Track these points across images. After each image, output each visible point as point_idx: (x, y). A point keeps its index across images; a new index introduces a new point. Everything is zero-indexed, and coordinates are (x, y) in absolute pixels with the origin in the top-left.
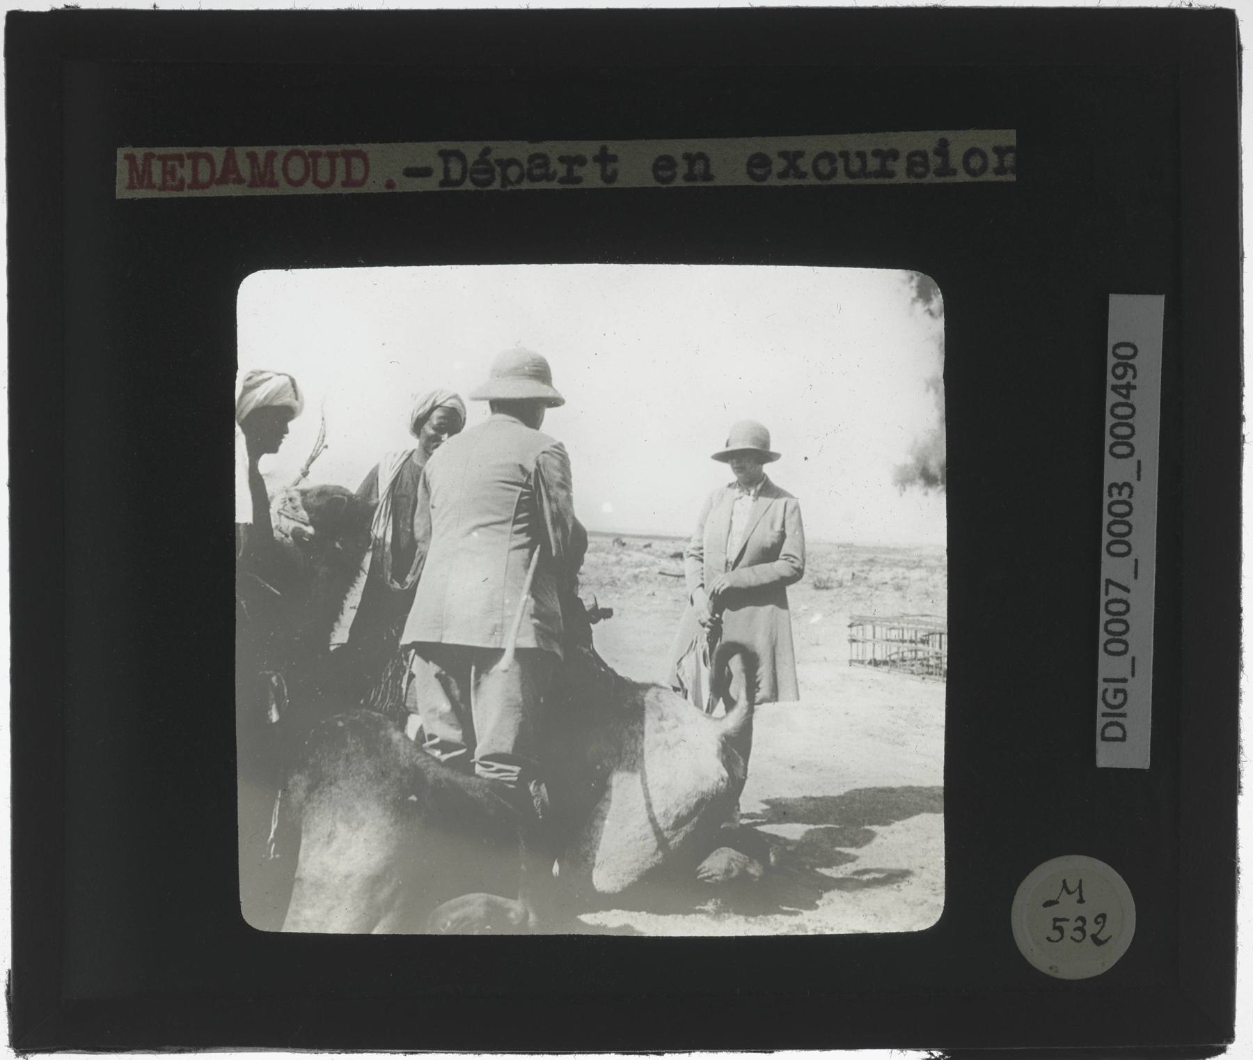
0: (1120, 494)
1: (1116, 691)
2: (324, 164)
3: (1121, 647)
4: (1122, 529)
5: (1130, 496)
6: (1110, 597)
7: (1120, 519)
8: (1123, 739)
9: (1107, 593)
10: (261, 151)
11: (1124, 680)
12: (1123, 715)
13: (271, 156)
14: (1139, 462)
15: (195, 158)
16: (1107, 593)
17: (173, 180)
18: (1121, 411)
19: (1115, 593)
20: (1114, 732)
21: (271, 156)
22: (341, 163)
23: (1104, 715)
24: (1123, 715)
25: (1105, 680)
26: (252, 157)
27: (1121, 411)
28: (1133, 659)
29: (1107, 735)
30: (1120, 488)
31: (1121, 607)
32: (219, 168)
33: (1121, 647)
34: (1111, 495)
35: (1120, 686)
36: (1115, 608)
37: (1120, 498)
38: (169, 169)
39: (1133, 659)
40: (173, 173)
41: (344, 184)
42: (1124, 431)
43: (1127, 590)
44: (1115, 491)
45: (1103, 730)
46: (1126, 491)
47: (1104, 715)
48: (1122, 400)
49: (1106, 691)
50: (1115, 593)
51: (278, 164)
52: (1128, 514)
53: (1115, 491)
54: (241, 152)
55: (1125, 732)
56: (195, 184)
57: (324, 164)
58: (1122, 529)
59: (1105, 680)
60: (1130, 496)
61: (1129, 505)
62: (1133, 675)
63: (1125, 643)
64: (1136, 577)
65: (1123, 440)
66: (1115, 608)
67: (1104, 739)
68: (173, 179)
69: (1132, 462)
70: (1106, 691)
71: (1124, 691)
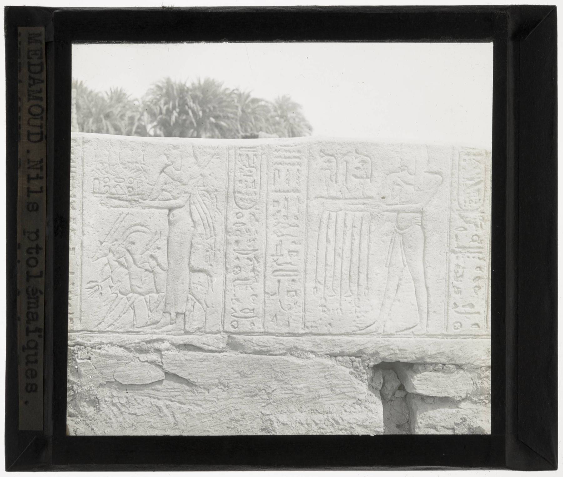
2: (38, 122)
10: (43, 95)
13: (41, 99)
15: (41, 64)
17: (32, 55)
21: (41, 99)
22: (38, 130)
26: (40, 91)
32: (37, 76)
38: (37, 52)
40: (36, 54)
41: (28, 132)
51: (38, 102)
54: (43, 86)
56: (29, 64)
57: (38, 122)
68: (32, 55)
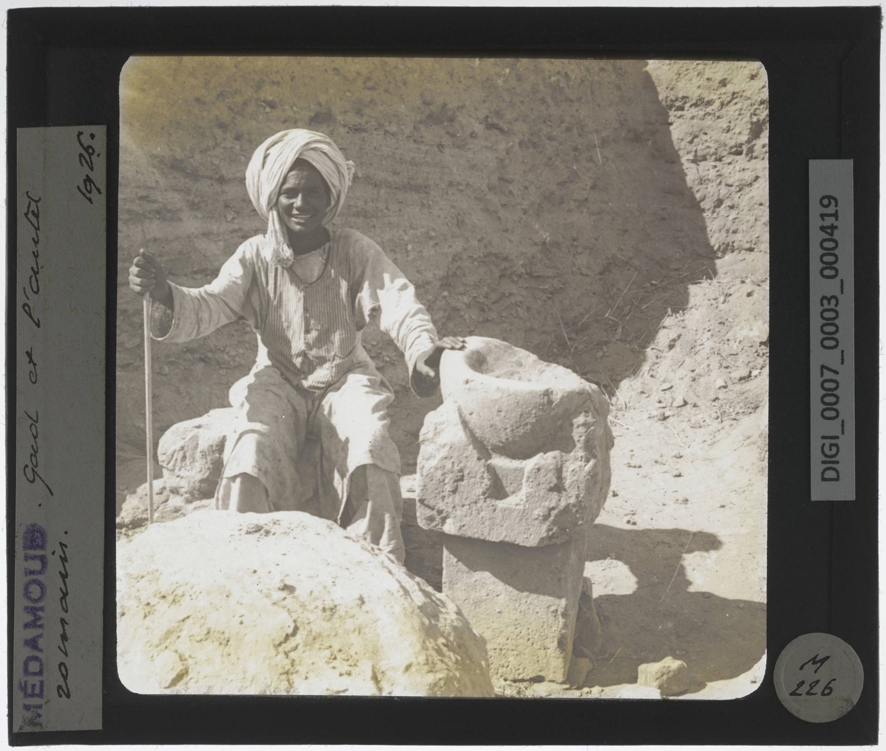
0: (829, 303)
1: (831, 445)
3: (833, 414)
4: (831, 329)
5: (836, 305)
6: (825, 378)
7: (830, 322)
8: (837, 479)
9: (822, 376)
11: (837, 437)
12: (837, 462)
14: (842, 281)
16: (822, 376)
18: (828, 245)
19: (828, 375)
20: (830, 474)
23: (823, 462)
24: (837, 462)
25: (823, 437)
27: (828, 245)
28: (843, 421)
29: (826, 476)
30: (829, 300)
31: (833, 385)
33: (833, 414)
34: (822, 305)
35: (833, 441)
36: (827, 385)
37: (828, 307)
39: (843, 421)
42: (831, 259)
43: (836, 372)
44: (825, 302)
45: (823, 473)
46: (833, 301)
47: (823, 462)
48: (829, 237)
49: (824, 445)
50: (828, 375)
52: (837, 317)
53: (825, 302)
55: (838, 476)
58: (831, 329)
59: (823, 437)
60: (836, 305)
61: (836, 312)
62: (843, 433)
63: (836, 411)
64: (842, 363)
65: (830, 266)
66: (827, 385)
67: (823, 479)
69: (837, 280)
70: (824, 445)
71: (836, 445)
